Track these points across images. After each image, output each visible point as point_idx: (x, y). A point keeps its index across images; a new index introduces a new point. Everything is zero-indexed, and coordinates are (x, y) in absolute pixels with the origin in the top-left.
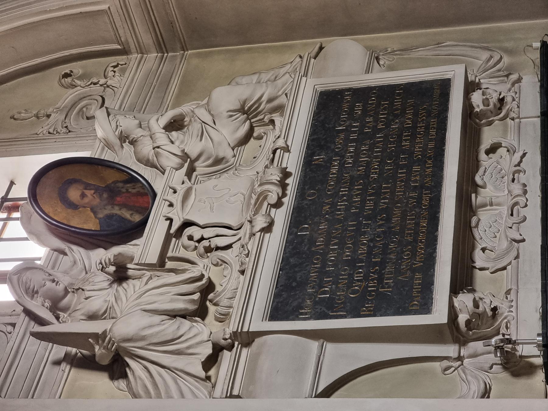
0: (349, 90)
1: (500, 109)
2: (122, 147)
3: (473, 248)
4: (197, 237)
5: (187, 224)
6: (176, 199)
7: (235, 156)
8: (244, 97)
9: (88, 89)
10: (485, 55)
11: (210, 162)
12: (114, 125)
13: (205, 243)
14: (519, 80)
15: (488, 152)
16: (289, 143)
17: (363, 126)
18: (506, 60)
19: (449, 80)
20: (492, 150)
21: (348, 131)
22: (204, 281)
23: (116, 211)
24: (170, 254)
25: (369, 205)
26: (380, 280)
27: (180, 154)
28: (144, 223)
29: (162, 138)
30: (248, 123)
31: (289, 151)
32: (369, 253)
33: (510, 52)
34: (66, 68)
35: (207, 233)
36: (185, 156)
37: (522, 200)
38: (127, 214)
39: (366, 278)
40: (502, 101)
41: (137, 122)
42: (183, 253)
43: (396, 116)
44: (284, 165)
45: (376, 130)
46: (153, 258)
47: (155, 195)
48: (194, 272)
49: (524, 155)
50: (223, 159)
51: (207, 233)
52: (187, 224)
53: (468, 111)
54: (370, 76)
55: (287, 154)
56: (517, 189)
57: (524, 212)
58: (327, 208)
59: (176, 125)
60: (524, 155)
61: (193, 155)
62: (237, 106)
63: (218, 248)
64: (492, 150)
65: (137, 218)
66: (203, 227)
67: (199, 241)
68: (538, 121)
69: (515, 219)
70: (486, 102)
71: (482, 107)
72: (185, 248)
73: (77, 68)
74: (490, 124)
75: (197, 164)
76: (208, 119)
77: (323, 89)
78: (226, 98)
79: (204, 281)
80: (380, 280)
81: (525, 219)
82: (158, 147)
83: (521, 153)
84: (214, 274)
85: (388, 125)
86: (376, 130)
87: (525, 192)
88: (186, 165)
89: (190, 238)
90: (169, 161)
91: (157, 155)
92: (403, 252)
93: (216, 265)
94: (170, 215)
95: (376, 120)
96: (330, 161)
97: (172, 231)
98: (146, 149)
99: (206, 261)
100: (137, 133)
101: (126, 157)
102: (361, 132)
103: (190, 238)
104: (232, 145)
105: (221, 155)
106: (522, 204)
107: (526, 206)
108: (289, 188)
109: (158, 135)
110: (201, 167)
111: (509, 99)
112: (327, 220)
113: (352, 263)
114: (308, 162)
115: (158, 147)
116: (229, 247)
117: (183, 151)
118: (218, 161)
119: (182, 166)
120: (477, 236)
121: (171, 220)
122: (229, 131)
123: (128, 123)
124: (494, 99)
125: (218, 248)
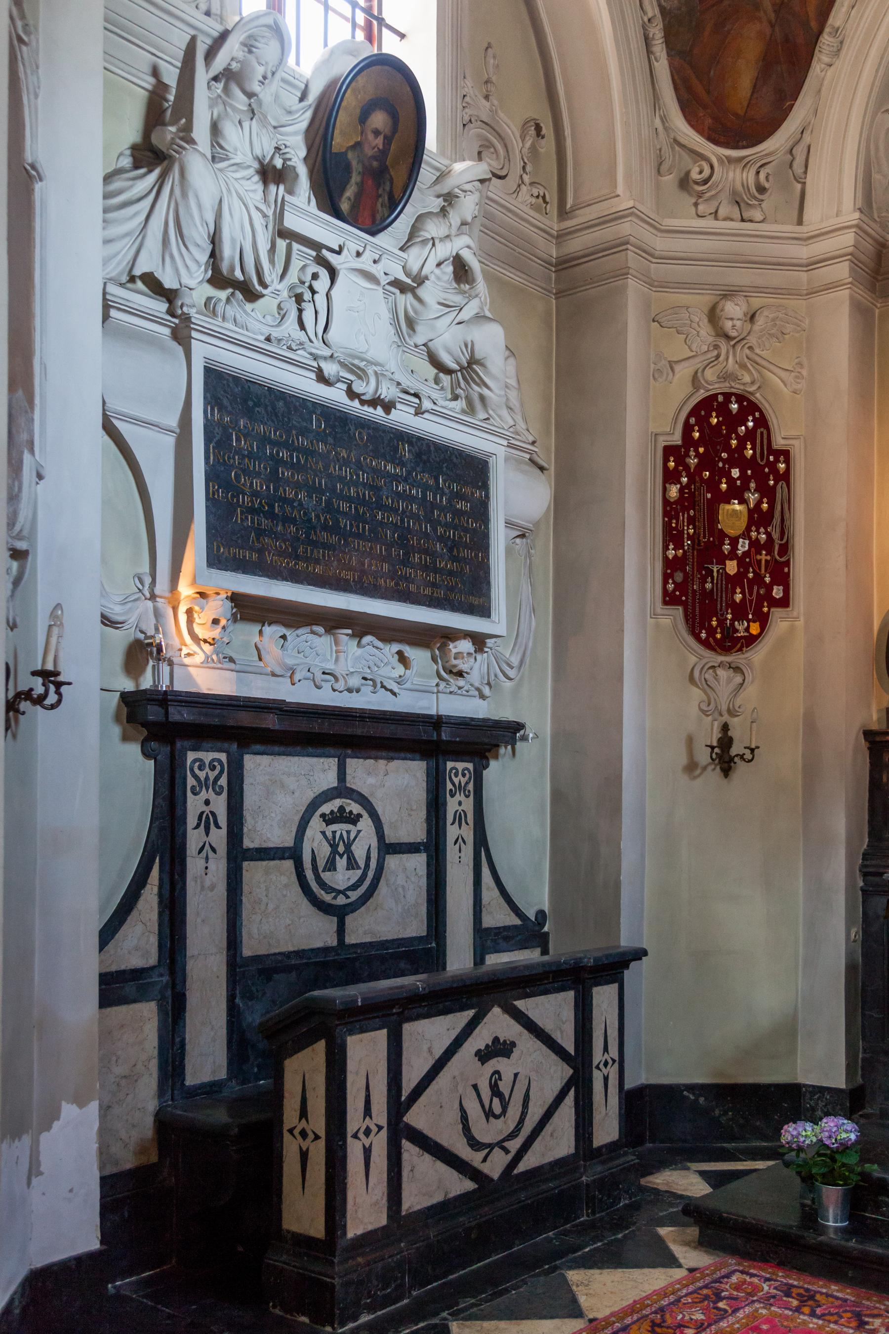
0: (487, 496)
1: (451, 672)
2: (438, 196)
3: (287, 625)
4: (316, 285)
5: (333, 274)
6: (365, 262)
7: (416, 346)
8: (489, 364)
9: (518, 156)
10: (515, 660)
11: (411, 313)
12: (467, 187)
13: (307, 296)
14: (482, 697)
15: (400, 653)
16: (426, 415)
17: (442, 509)
18: (508, 684)
19: (489, 616)
20: (403, 659)
21: (437, 489)
22: (259, 288)
23: (355, 178)
24: (296, 246)
25: (344, 506)
26: (252, 511)
27: (424, 273)
28: (337, 214)
29: (444, 250)
30: (455, 366)
31: (416, 414)
32: (284, 500)
33: (515, 691)
34: (548, 130)
35: (320, 299)
36: (420, 280)
37: (340, 685)
38: (350, 192)
39: (255, 494)
40: (460, 674)
41: (469, 219)
42: (296, 264)
43: (451, 550)
44: (398, 406)
45: (435, 523)
46: (291, 222)
47: (373, 234)
48: (271, 275)
49: (394, 694)
50: (414, 330)
51: (320, 299)
52: (333, 274)
53: (449, 635)
54: (502, 524)
55: (412, 411)
56: (355, 681)
57: (327, 686)
58: (344, 454)
59: (461, 271)
60: (394, 694)
61: (421, 292)
62: (478, 355)
63: (300, 311)
64: (403, 659)
65: (345, 206)
66: (328, 296)
67: (311, 288)
68: (433, 712)
69: (319, 676)
70: (458, 656)
71: (454, 651)
72: (303, 268)
73: (548, 146)
74: (434, 659)
75: (409, 296)
76: (466, 315)
77: (491, 465)
78: (490, 340)
79: (259, 288)
80: (252, 511)
81: (319, 687)
82: (434, 245)
83: (396, 690)
84: (268, 303)
85: (441, 539)
86: (435, 523)
87: (350, 690)
88: (409, 281)
89: (315, 276)
90: (415, 258)
91: (424, 242)
92: (284, 541)
93: (279, 307)
94: (345, 252)
95: (447, 526)
96: (402, 464)
97: (324, 252)
98: (433, 229)
99: (285, 294)
100: (455, 218)
101: (422, 200)
102: (433, 506)
103: (315, 276)
104: (430, 344)
105: (419, 328)
106: (336, 686)
107: (334, 690)
108: (371, 410)
109: (448, 245)
110: (405, 301)
111: (461, 682)
112: (329, 452)
113: (274, 477)
114: (401, 436)
115: (434, 245)
116: (302, 327)
117: (427, 278)
118: (411, 324)
119: (408, 275)
120: (300, 631)
121: (339, 253)
122: (447, 339)
123: (468, 206)
124: (463, 666)
125: (300, 311)
